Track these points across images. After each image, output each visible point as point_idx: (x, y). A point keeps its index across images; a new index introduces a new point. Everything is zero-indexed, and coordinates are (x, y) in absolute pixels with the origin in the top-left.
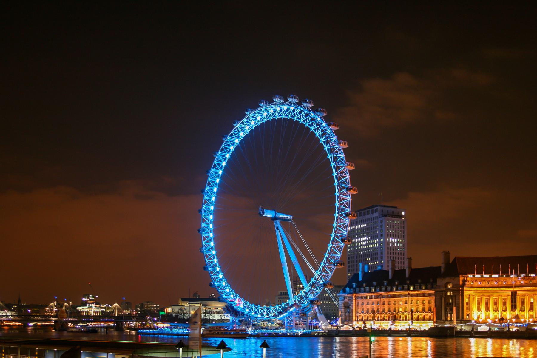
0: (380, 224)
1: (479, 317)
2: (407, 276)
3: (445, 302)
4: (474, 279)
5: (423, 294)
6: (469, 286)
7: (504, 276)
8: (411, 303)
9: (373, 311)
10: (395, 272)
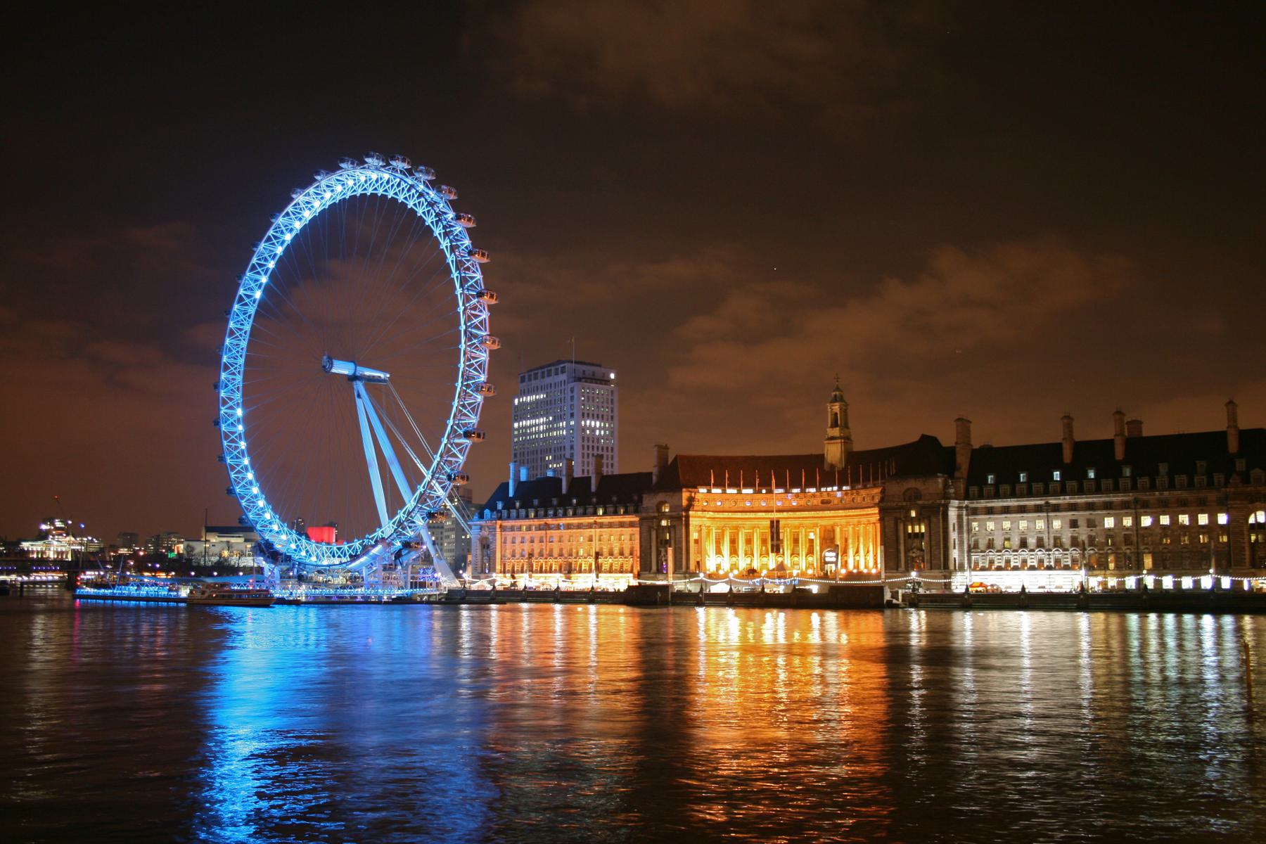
0: (570, 394)
1: (718, 567)
2: (593, 488)
3: (657, 537)
4: (709, 496)
7: (764, 491)
8: (600, 540)
9: (531, 555)
10: (573, 482)
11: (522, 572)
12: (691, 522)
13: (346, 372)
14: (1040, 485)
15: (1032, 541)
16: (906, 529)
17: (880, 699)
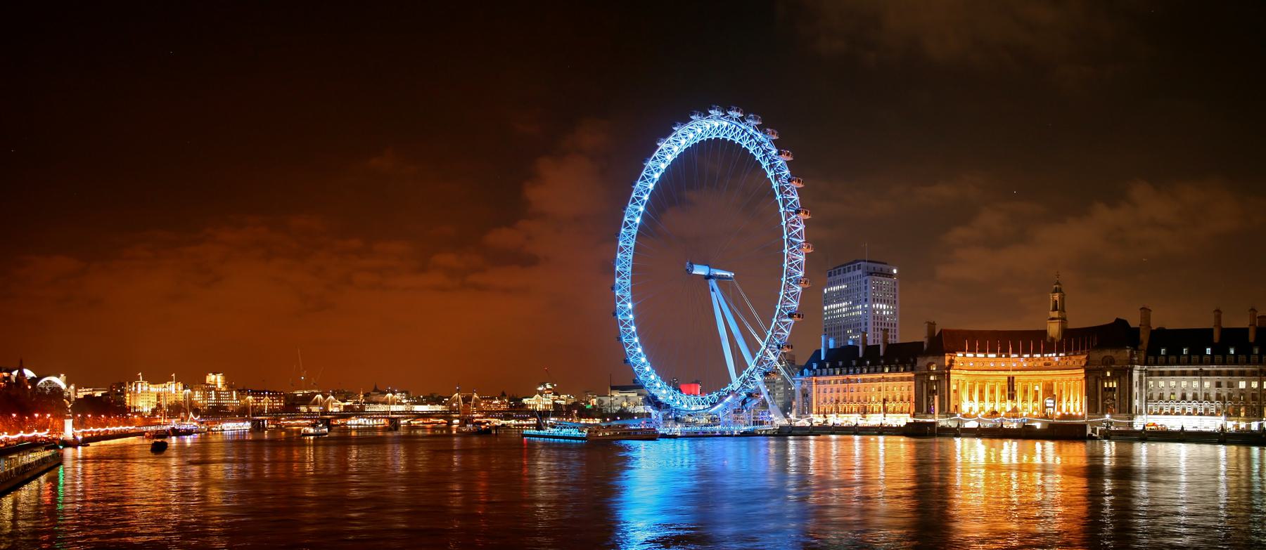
1: (971, 409)
2: (882, 353)
3: (927, 388)
4: (964, 359)
5: (901, 378)
6: (958, 368)
7: (1003, 356)
9: (837, 401)
11: (831, 413)
12: (951, 378)
13: (703, 273)
14: (1197, 357)
15: (1189, 396)
16: (1103, 385)
17: (1083, 503)
